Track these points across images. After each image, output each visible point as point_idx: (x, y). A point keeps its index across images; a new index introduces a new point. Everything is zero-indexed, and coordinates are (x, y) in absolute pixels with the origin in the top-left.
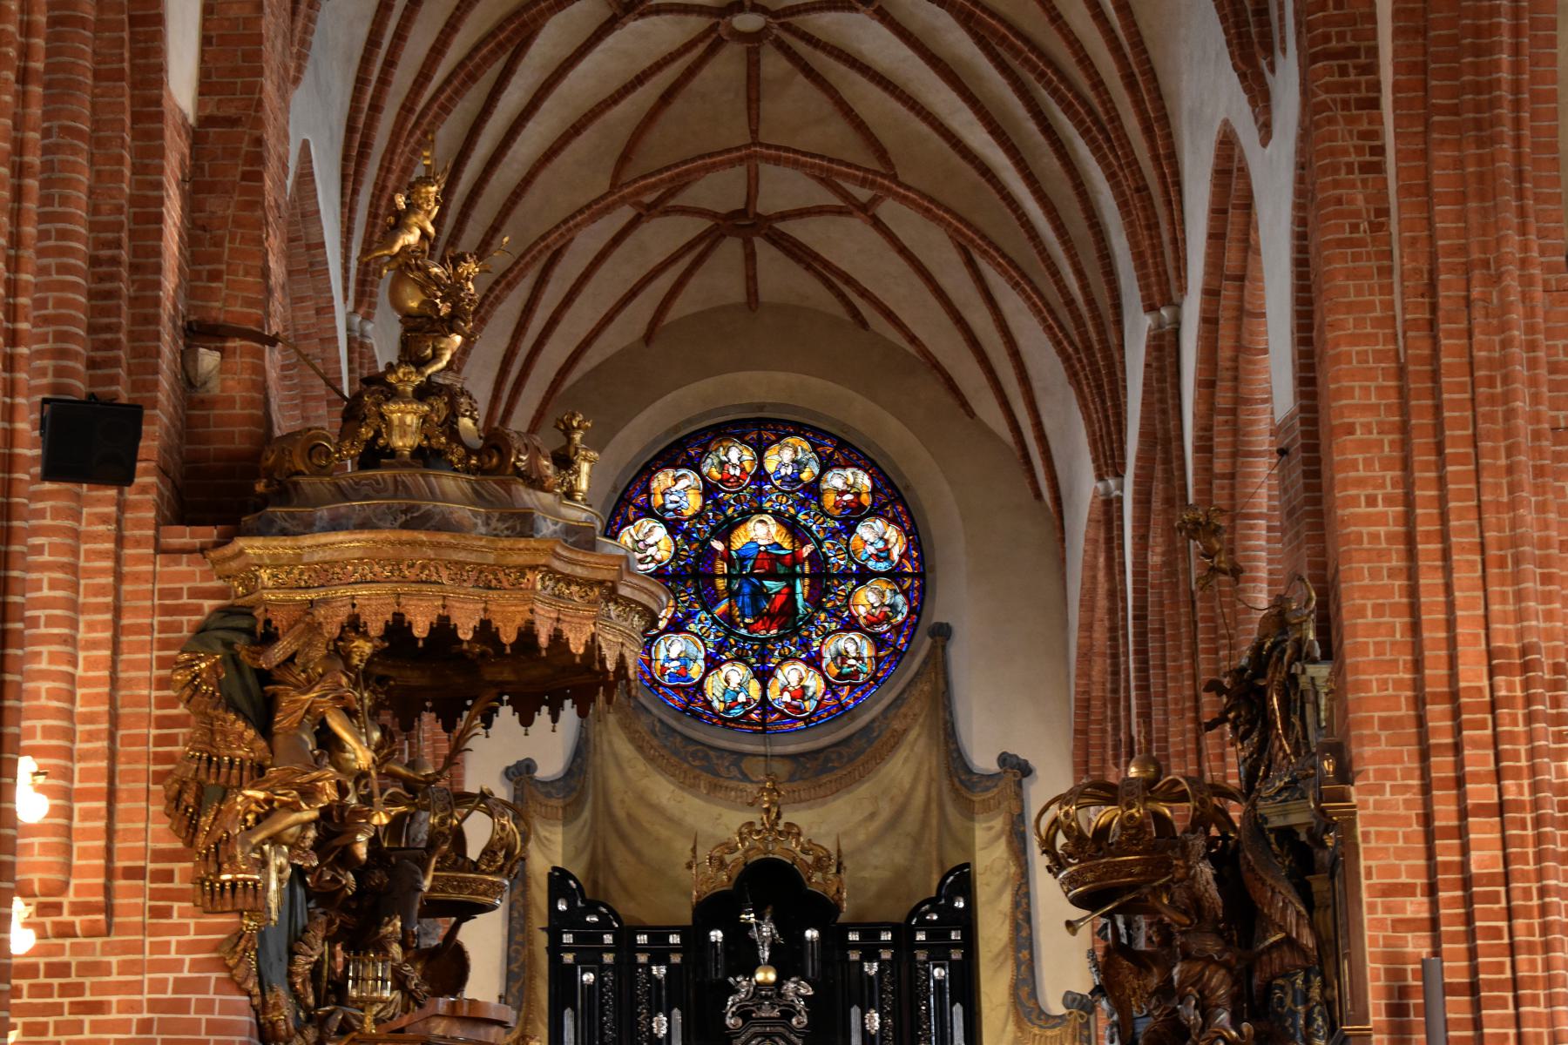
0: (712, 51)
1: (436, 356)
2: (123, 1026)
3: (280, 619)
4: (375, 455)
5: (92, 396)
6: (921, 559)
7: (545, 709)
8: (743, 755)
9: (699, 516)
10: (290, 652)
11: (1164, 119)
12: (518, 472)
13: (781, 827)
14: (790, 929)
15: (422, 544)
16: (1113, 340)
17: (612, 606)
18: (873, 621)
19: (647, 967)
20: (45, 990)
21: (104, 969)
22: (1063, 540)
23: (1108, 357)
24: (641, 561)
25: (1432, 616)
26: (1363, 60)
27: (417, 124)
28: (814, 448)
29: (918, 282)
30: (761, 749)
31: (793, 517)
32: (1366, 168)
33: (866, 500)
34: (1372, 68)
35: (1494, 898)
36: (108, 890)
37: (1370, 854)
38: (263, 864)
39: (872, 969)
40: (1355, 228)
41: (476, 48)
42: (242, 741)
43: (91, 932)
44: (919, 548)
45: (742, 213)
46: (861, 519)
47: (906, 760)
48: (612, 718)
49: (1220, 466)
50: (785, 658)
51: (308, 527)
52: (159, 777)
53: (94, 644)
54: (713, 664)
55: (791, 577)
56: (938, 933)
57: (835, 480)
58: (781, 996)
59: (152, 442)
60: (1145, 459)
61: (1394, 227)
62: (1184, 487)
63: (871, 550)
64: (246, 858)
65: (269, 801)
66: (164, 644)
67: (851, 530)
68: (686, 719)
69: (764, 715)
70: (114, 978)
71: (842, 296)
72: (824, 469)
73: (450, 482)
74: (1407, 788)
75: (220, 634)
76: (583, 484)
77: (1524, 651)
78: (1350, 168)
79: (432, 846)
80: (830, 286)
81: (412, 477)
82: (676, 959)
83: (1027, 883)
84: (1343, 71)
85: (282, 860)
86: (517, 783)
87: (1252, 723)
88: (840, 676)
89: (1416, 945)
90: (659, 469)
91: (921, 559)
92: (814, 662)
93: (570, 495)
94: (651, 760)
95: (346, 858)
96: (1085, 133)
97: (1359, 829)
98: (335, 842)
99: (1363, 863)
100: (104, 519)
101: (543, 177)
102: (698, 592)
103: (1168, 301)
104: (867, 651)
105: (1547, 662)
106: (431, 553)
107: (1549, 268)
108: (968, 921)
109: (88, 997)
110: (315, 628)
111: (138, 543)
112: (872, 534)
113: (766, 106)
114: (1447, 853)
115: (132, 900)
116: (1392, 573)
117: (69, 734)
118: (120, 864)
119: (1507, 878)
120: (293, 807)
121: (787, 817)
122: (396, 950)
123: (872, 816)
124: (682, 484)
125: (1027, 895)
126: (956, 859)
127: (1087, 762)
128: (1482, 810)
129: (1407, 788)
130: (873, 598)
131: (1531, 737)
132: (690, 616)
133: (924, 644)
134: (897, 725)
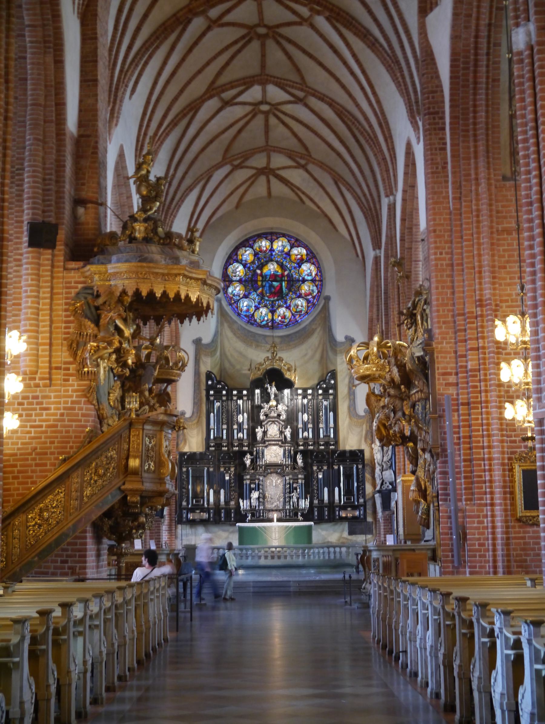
0: (254, 116)
1: (151, 209)
2: (56, 415)
3: (101, 291)
4: (132, 239)
5: (43, 221)
6: (321, 276)
7: (187, 319)
8: (265, 336)
9: (253, 262)
10: (104, 300)
11: (391, 137)
12: (175, 244)
13: (277, 358)
14: (280, 388)
15: (144, 267)
16: (378, 207)
17: (205, 286)
18: (306, 295)
20: (32, 404)
21: (50, 397)
23: (376, 212)
24: (235, 276)
26: (440, 115)
27: (159, 139)
28: (289, 241)
29: (321, 190)
30: (271, 334)
31: (282, 263)
33: (305, 257)
34: (443, 118)
36: (50, 373)
37: (438, 363)
38: (98, 366)
39: (305, 401)
40: (437, 168)
41: (177, 115)
42: (90, 328)
43: (45, 386)
44: (320, 272)
45: (265, 168)
46: (302, 263)
48: (226, 325)
49: (406, 245)
50: (280, 306)
51: (110, 262)
52: (65, 339)
53: (45, 298)
54: (257, 308)
55: (281, 281)
56: (326, 391)
57: (295, 251)
59: (62, 235)
60: (386, 244)
62: (397, 252)
63: (306, 273)
64: (91, 364)
65: (98, 346)
66: (67, 298)
67: (300, 267)
68: (249, 325)
69: (273, 323)
70: (52, 400)
71: (297, 194)
72: (292, 248)
73: (154, 248)
75: (84, 295)
76: (197, 249)
78: (436, 149)
79: (157, 362)
80: (293, 191)
81: (143, 247)
84: (434, 119)
85: (105, 365)
87: (412, 324)
88: (296, 312)
90: (241, 248)
91: (321, 276)
92: (288, 308)
93: (193, 252)
94: (238, 337)
95: (125, 365)
96: (367, 141)
97: (435, 355)
98: (122, 359)
99: (436, 366)
100: (48, 260)
101: (201, 156)
102: (252, 286)
103: (392, 194)
104: (305, 304)
105: (493, 303)
106: (147, 270)
107: (497, 181)
108: (335, 387)
109: (44, 406)
110: (111, 293)
111: (58, 267)
112: (308, 269)
113: (271, 134)
115: (58, 376)
116: (448, 276)
117: (38, 326)
118: (54, 365)
120: (105, 348)
121: (279, 355)
122: (147, 393)
123: (306, 355)
124: (248, 252)
126: (332, 368)
128: (472, 349)
129: (450, 343)
130: (306, 288)
132: (250, 293)
133: (322, 302)
134: (314, 327)
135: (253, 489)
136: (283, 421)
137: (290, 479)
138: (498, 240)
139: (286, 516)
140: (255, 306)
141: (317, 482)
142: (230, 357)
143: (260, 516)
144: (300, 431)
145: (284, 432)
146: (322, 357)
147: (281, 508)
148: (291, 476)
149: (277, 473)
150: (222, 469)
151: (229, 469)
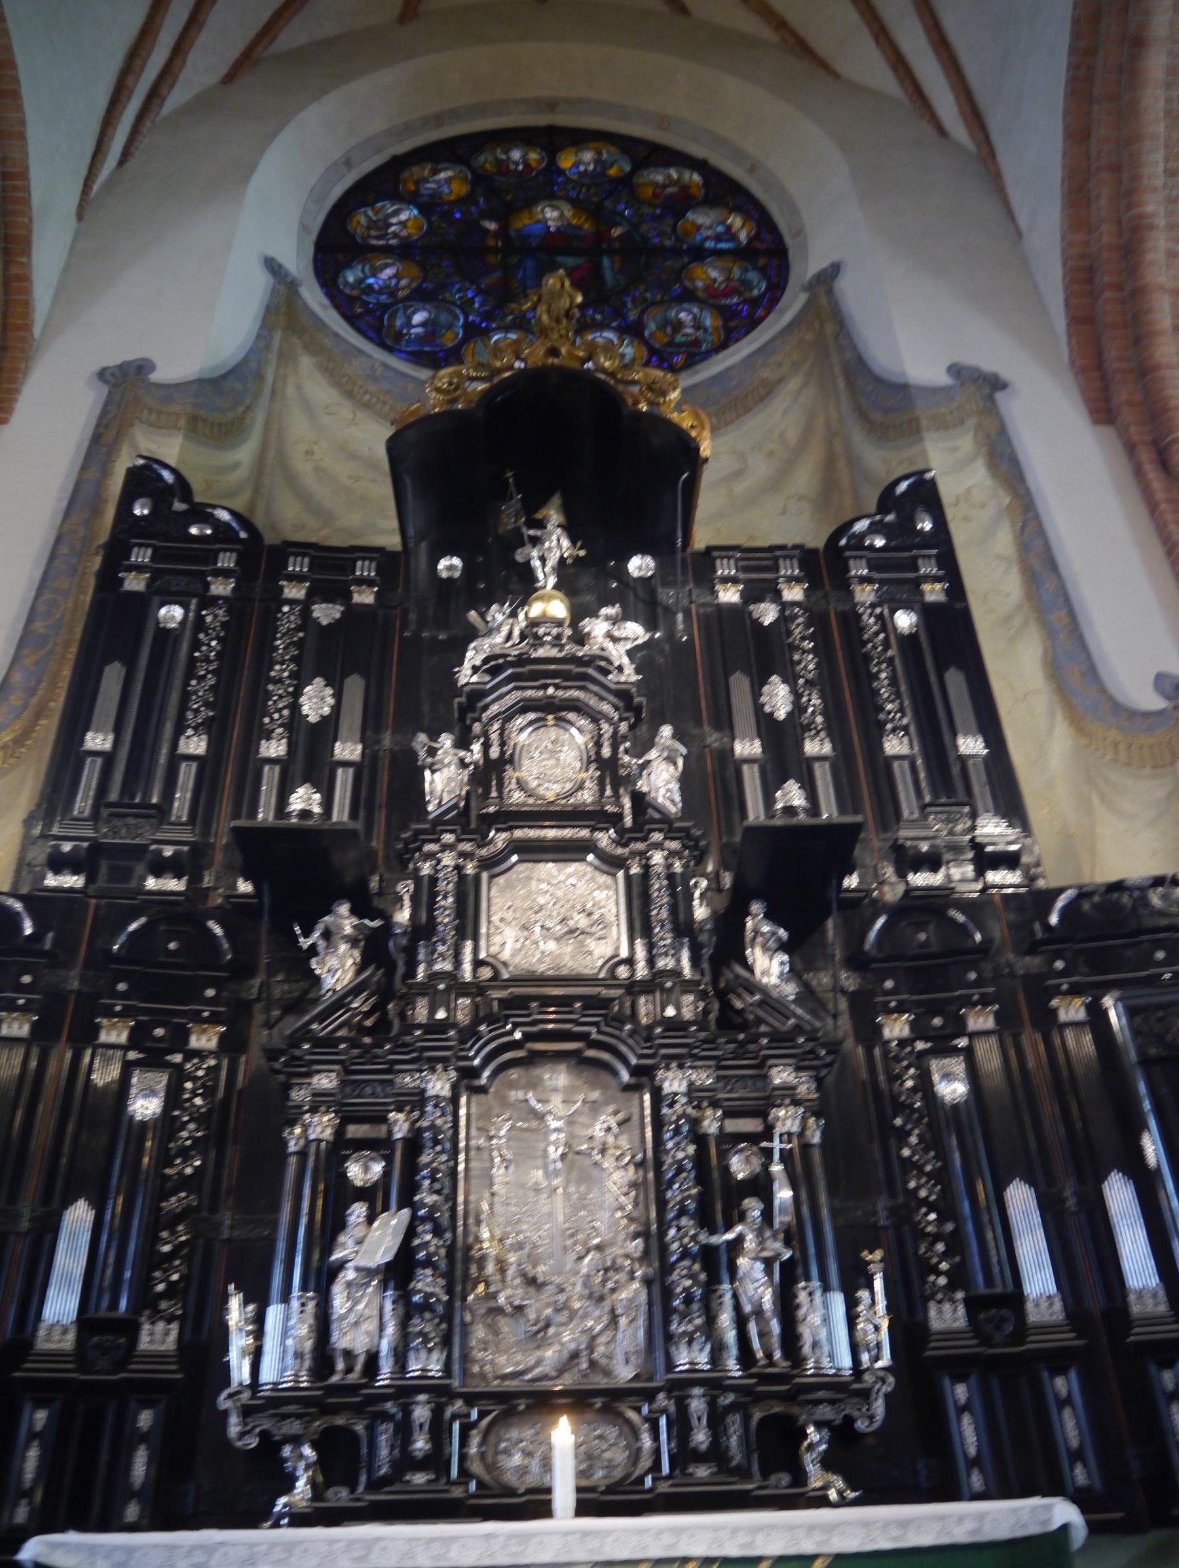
19: (305, 606)
22: (992, 155)
24: (378, 238)
47: (786, 412)
48: (306, 362)
58: (580, 639)
82: (365, 597)
83: (1037, 517)
86: (115, 386)
88: (670, 344)
94: (367, 406)
123: (738, 474)
124: (443, 175)
125: (1041, 532)
127: (1099, 365)
134: (766, 373)
135: (364, 1194)
136: (623, 695)
137: (692, 1091)
139: (684, 1456)
140: (467, 326)
141: (933, 1142)
142: (309, 480)
143: (405, 1462)
144: (751, 779)
145: (630, 780)
146: (829, 465)
147: (624, 1373)
148: (704, 1078)
149: (578, 1061)
150: (114, 1034)
151: (179, 1039)
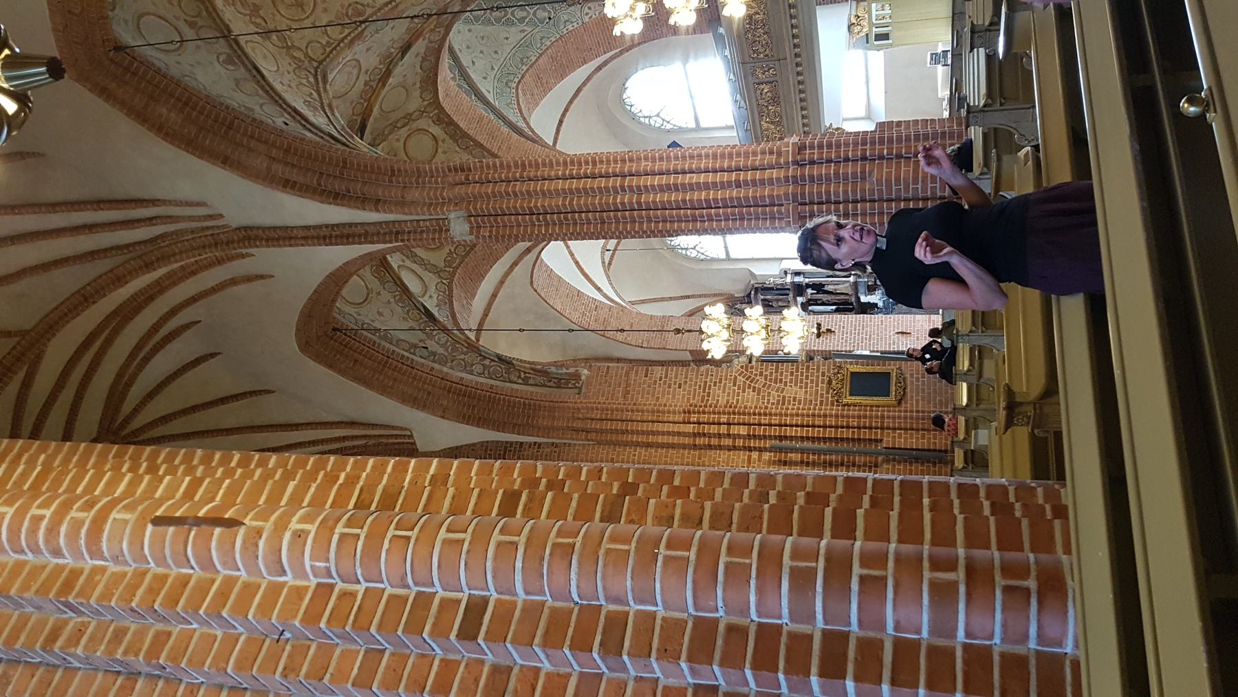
25: (670, 439)
32: (539, 448)
34: (511, 443)
35: (755, 429)
40: (555, 452)
61: (558, 441)
74: (719, 454)
77: (685, 412)
89: (766, 456)
107: (579, 398)
114: (739, 442)
116: (656, 452)
119: (750, 425)
128: (728, 430)
129: (719, 454)
131: (709, 413)
138: (632, 400)
